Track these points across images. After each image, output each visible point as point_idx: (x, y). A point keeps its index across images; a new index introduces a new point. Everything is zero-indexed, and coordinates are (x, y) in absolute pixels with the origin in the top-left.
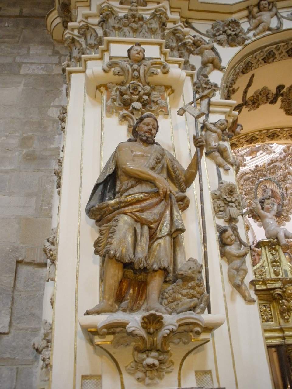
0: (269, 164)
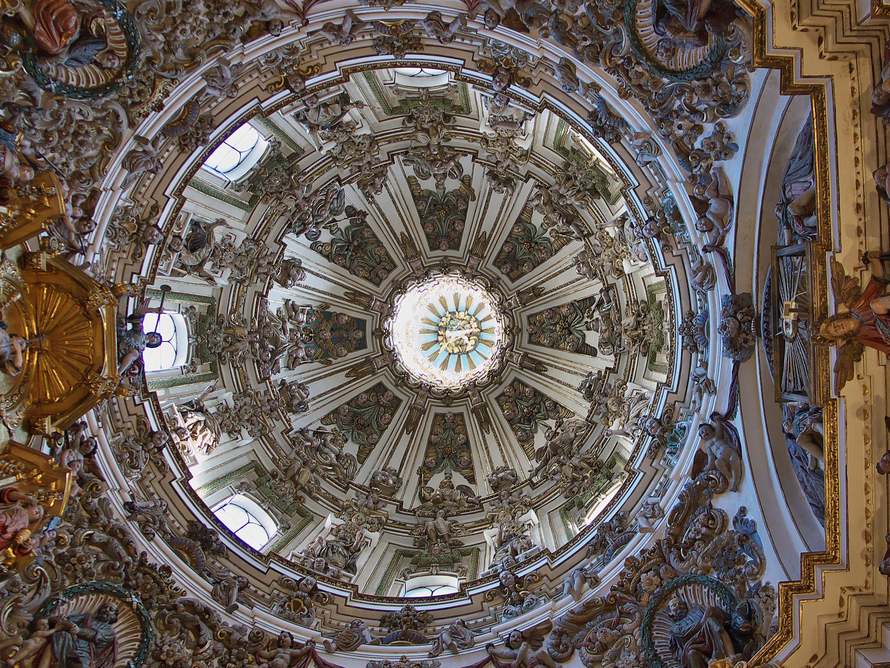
0: (191, 606)
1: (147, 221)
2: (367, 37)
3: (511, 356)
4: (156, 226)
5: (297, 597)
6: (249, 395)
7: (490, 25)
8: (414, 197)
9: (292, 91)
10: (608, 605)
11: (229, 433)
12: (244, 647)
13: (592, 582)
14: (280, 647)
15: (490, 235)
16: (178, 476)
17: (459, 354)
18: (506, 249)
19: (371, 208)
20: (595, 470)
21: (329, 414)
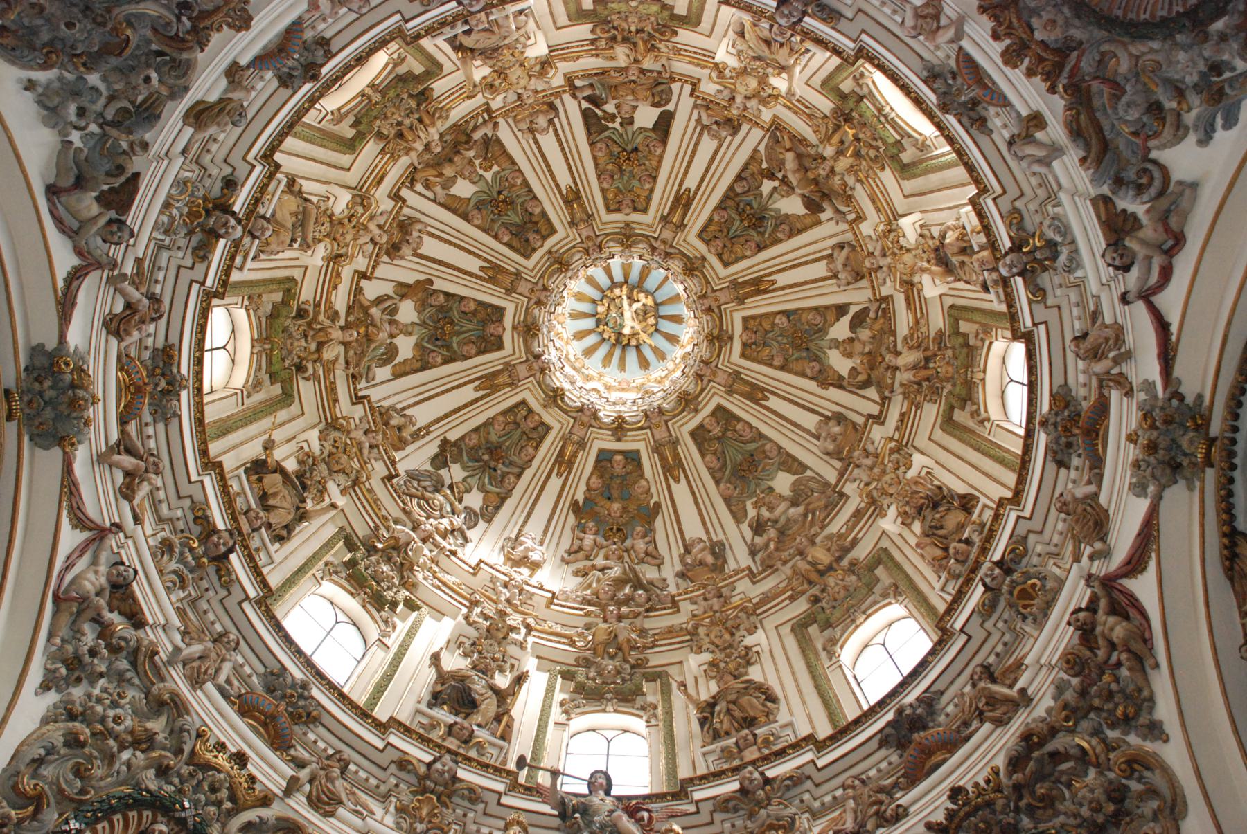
0: (1015, 763)
1: (421, 779)
2: (150, 431)
3: (664, 242)
4: (429, 765)
5: (1011, 593)
6: (696, 627)
7: (126, 236)
8: (423, 369)
9: (231, 550)
10: (1079, 96)
11: (749, 663)
12: (1090, 685)
13: (1036, 126)
14: (1093, 629)
15: (485, 260)
16: (809, 756)
17: (658, 317)
18: (506, 239)
19: (437, 431)
20: (846, 120)
21: (731, 511)
